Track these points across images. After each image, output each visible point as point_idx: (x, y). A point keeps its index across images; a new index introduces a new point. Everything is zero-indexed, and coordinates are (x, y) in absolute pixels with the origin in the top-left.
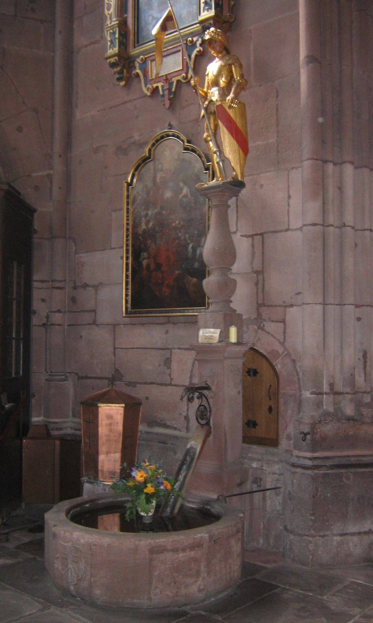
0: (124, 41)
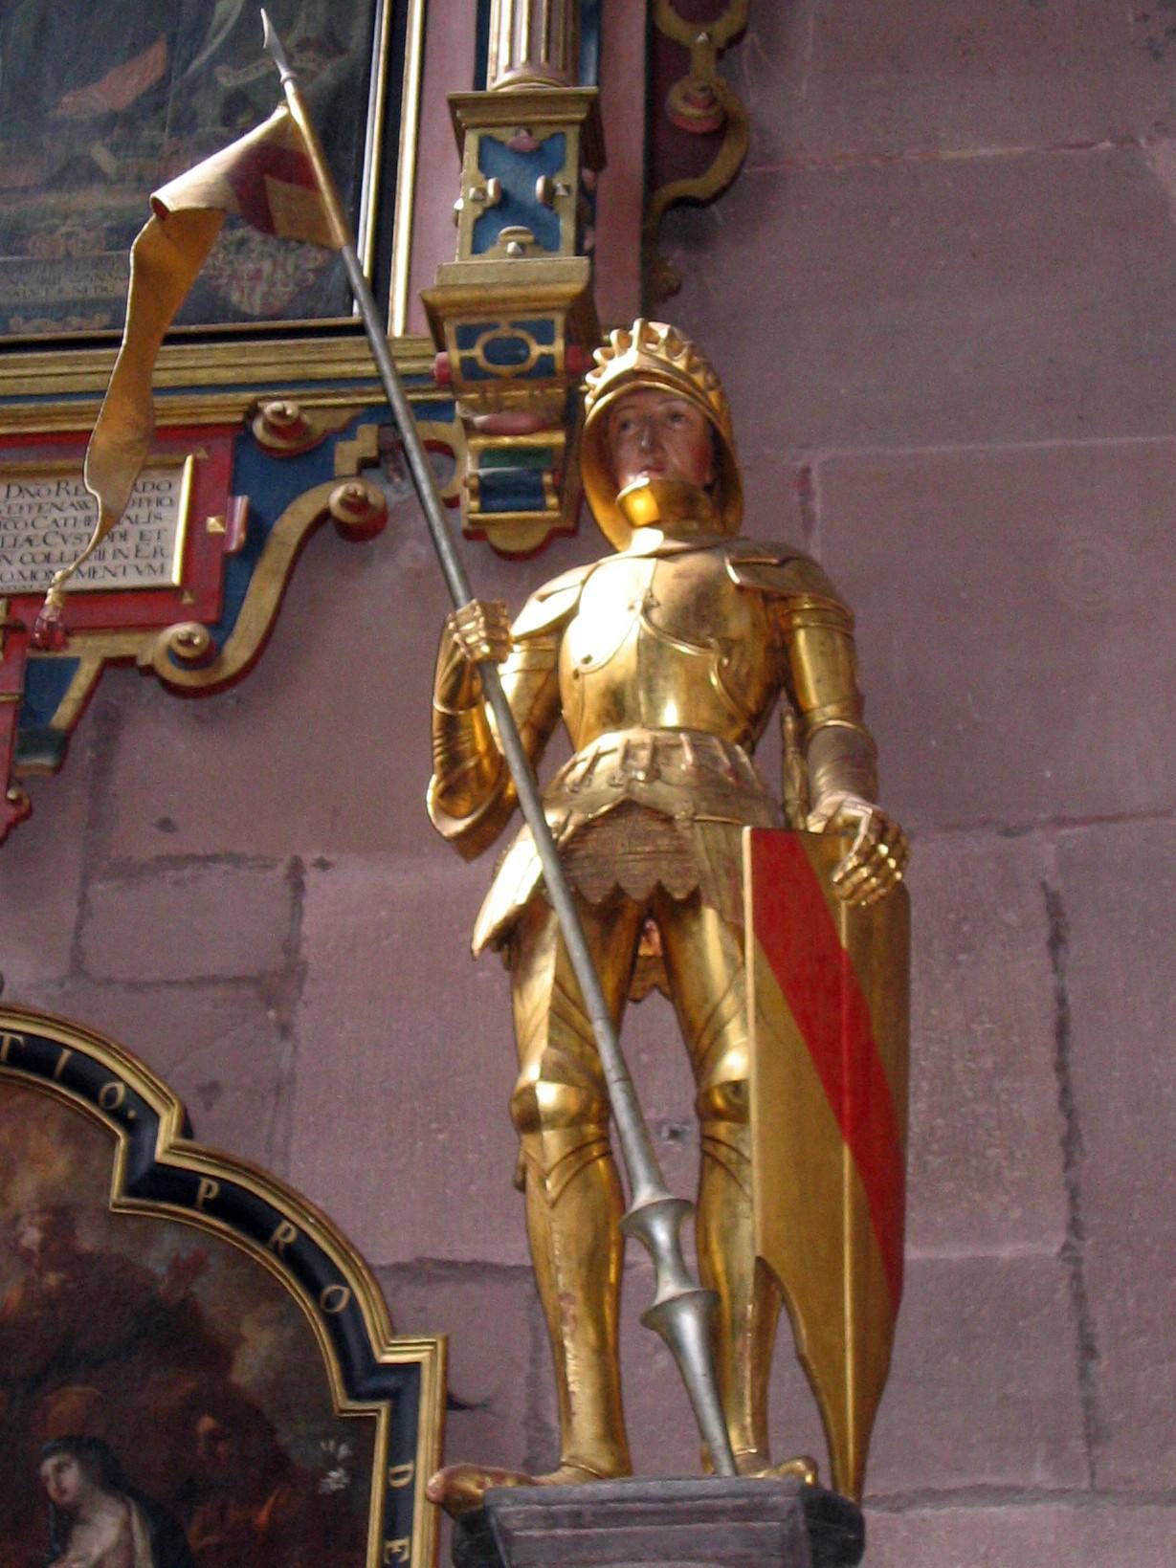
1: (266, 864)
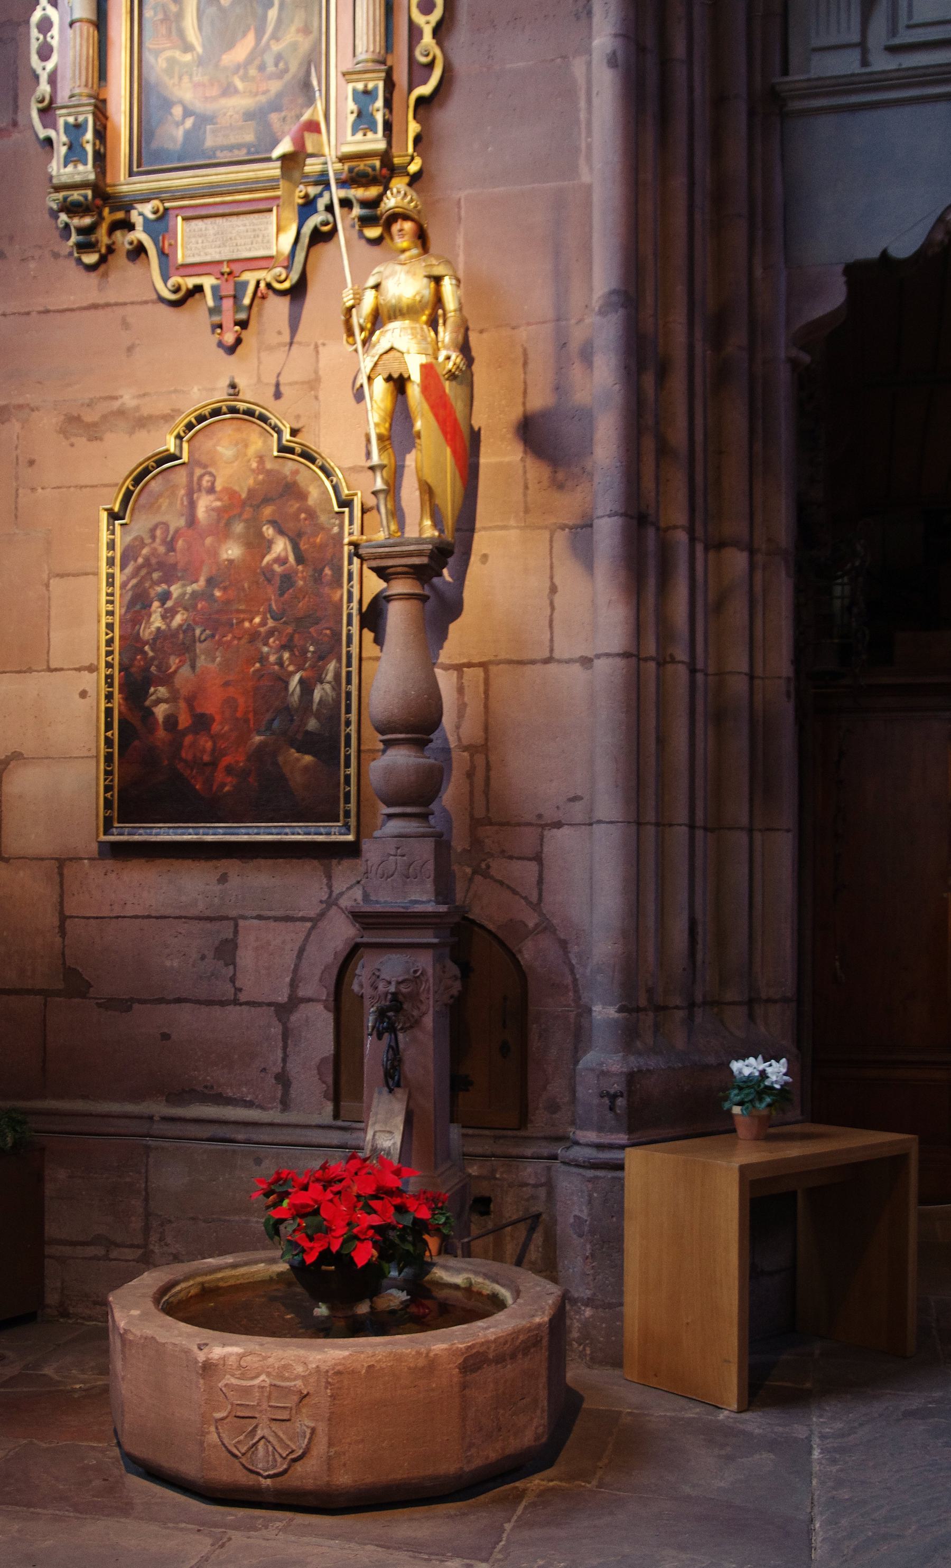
0: (102, 150)
1: (308, 345)
